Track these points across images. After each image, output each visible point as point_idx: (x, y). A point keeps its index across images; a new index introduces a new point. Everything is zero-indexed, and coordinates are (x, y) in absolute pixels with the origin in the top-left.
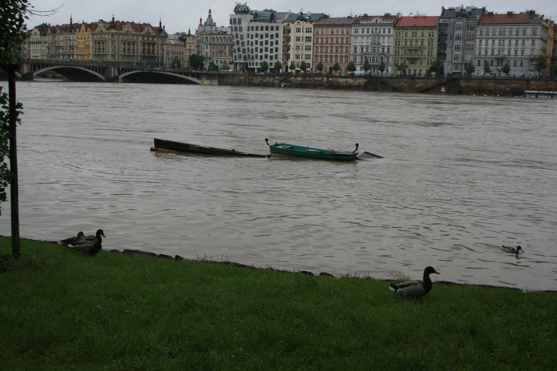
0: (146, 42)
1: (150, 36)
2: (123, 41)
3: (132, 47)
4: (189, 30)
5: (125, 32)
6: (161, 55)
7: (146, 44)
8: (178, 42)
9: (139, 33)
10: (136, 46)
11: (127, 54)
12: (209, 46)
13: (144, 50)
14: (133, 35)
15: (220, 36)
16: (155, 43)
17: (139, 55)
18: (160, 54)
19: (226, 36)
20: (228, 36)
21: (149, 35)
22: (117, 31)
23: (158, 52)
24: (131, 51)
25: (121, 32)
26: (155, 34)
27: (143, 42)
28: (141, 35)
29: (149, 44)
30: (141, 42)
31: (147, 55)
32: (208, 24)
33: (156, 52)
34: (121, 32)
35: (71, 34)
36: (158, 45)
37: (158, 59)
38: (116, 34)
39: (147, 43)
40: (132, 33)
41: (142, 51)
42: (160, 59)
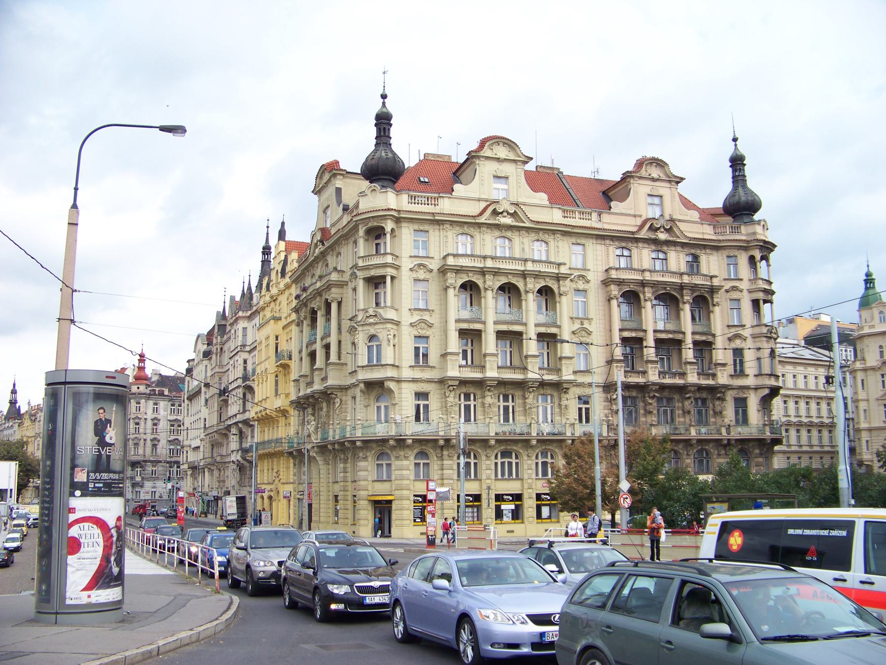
0: (643, 284)
1: (667, 243)
2: (459, 270)
4: (868, 275)
5: (473, 209)
6: (759, 375)
7: (649, 293)
9: (593, 222)
10: (566, 306)
11: (492, 373)
13: (633, 344)
14: (542, 230)
16: (713, 290)
18: (750, 367)
21: (662, 236)
23: (738, 353)
25: (446, 206)
26: (707, 232)
27: (620, 282)
28: (602, 237)
30: (606, 283)
31: (653, 376)
33: (722, 354)
34: (446, 206)
37: (741, 404)
38: (398, 220)
39: (654, 285)
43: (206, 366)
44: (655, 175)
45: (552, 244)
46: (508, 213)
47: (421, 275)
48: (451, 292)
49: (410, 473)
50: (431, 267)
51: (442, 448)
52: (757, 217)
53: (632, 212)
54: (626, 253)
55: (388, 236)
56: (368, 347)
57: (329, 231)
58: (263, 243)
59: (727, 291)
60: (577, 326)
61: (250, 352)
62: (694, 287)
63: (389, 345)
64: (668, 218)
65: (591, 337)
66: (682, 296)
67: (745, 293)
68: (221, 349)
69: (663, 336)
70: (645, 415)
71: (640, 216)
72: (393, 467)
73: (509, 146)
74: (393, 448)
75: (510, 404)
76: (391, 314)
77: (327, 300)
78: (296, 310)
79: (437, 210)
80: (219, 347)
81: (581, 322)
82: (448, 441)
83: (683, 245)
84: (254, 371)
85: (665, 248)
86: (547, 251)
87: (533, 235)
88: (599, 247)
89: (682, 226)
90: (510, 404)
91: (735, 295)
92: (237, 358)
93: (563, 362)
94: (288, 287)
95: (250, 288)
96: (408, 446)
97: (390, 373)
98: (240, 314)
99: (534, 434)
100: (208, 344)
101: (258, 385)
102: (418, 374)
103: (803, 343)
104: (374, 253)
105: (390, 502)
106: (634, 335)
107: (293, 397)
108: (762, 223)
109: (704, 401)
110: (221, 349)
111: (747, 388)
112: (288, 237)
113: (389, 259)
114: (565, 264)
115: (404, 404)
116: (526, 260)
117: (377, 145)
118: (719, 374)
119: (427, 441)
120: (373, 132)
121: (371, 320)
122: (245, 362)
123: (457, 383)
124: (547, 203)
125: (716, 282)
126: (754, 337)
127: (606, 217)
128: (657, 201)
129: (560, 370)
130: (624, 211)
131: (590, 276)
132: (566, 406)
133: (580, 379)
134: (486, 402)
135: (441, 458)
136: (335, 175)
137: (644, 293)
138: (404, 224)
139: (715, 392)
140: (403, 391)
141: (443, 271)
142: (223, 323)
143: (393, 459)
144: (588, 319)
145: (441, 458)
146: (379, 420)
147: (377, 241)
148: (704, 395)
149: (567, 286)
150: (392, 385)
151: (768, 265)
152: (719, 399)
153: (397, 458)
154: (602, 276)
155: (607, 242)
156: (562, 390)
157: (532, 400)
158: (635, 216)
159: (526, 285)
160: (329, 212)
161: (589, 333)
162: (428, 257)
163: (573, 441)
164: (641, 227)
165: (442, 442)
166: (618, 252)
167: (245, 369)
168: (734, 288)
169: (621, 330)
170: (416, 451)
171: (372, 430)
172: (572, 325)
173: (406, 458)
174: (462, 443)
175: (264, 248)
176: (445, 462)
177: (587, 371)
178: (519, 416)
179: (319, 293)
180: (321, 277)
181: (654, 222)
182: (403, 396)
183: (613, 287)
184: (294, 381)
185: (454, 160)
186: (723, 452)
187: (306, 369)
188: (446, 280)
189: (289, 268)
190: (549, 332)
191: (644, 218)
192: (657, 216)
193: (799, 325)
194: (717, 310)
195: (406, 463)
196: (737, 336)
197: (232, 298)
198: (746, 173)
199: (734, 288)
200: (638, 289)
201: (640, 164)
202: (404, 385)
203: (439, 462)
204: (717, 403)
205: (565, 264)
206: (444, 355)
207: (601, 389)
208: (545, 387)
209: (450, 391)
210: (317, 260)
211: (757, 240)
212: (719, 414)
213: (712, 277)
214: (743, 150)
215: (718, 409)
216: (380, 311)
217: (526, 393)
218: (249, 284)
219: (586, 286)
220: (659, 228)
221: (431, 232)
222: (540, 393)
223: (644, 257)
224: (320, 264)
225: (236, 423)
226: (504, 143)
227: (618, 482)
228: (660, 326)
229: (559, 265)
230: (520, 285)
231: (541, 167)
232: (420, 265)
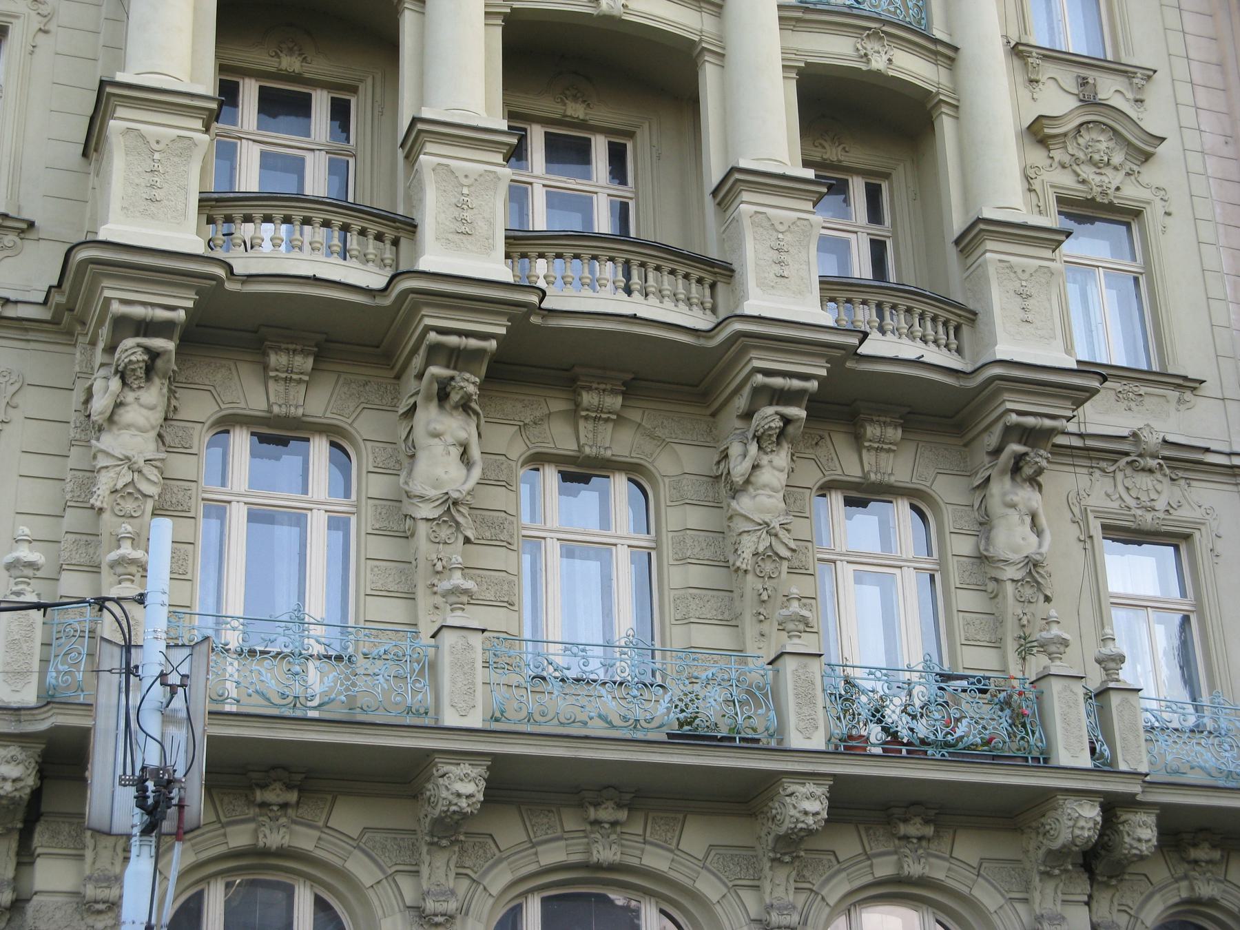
65: (1152, 174)
81: (1084, 82)
93: (993, 253)
129: (972, 317)
132: (1033, 565)
134: (417, 487)
156: (997, 452)
157: (777, 502)
163: (1113, 806)
172: (1024, 93)
178: (686, 622)
190: (878, 63)
208: (872, 431)
209: (123, 376)
217: (735, 450)
222: (836, 475)
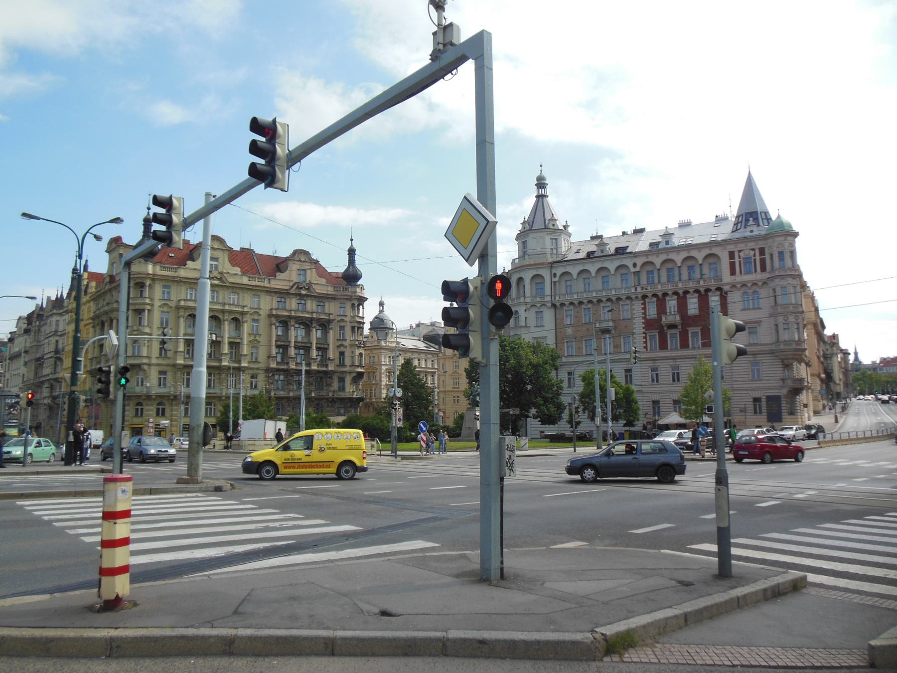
0: (290, 317)
1: (306, 295)
3: (227, 330)
8: (421, 345)
10: (246, 328)
12: (548, 316)
13: (283, 347)
14: (236, 288)
15: (598, 265)
16: (329, 321)
17: (261, 366)
18: (348, 361)
19: (629, 263)
20: (640, 261)
21: (304, 292)
22: (159, 271)
23: (342, 354)
24: (226, 349)
25: (182, 273)
26: (330, 290)
27: (277, 316)
28: (270, 292)
29: (306, 324)
30: (270, 316)
32: (538, 225)
34: (182, 273)
35: (61, 314)
36: (342, 328)
37: (342, 380)
38: (153, 280)
40: (231, 280)
41: (274, 351)
42: (348, 379)
43: (26, 339)
44: (302, 259)
45: (241, 294)
46: (217, 278)
47: (165, 309)
48: (182, 320)
49: (154, 413)
50: (171, 305)
51: (172, 400)
52: (359, 283)
53: (288, 279)
54: (283, 300)
55: (147, 288)
56: (133, 346)
57: (115, 279)
58: (73, 266)
59: (338, 321)
60: (252, 338)
61: (61, 336)
62: (318, 320)
63: (144, 346)
64: (308, 282)
66: (312, 324)
67: (348, 323)
68: (39, 330)
69: (300, 345)
70: (287, 385)
71: (292, 281)
72: (144, 410)
73: (221, 241)
74: (145, 400)
75: (213, 378)
76: (147, 330)
77: (110, 317)
78: (93, 319)
79: (176, 274)
80: (37, 328)
82: (175, 397)
83: (315, 297)
84: (63, 349)
85: (305, 298)
86: (238, 298)
87: (231, 289)
88: (267, 297)
89: (314, 286)
90: (213, 378)
91: (342, 324)
92: (51, 339)
94: (88, 302)
95: (62, 295)
96: (154, 399)
97: (145, 361)
98: (55, 311)
99: (224, 394)
100: (28, 324)
101: (66, 358)
102: (161, 361)
103: (422, 339)
104: (139, 296)
105: (141, 428)
106: (283, 343)
107: (89, 369)
108: (361, 286)
109: (321, 378)
110: (39, 330)
111: (345, 372)
112: (90, 270)
113: (147, 301)
114: (247, 306)
115: (152, 377)
116: (225, 304)
117: (144, 236)
118: (329, 365)
119: (164, 396)
120: (142, 228)
121: (135, 333)
122: (57, 342)
123: (182, 367)
124: (240, 273)
125: (332, 317)
126: (351, 346)
127: (273, 282)
128: (302, 272)
130: (283, 278)
131: (261, 312)
133: (252, 366)
135: (172, 405)
136: (119, 246)
137: (290, 322)
138: (157, 282)
139: (328, 374)
140: (152, 370)
141: (178, 308)
142: (41, 313)
143: (144, 405)
144: (258, 334)
145: (172, 405)
146: (138, 385)
147: (141, 289)
148: (322, 375)
149: (247, 318)
150: (145, 367)
151: (363, 308)
152: (329, 377)
153: (147, 405)
154: (268, 313)
155: (273, 294)
158: (289, 281)
159: (224, 317)
160: (115, 265)
161: (259, 342)
162: (170, 300)
164: (292, 287)
165: (172, 397)
166: (279, 300)
167: (57, 346)
168: (342, 320)
169: (276, 341)
170: (157, 402)
171: (133, 390)
173: (152, 405)
174: (182, 398)
175: (73, 269)
176: (174, 408)
177: (256, 362)
179: (106, 313)
180: (108, 304)
181: (300, 284)
182: (152, 372)
183: (273, 319)
184: (90, 359)
185: (191, 242)
186: (330, 405)
187: (96, 354)
188: (179, 313)
189: (89, 291)
191: (294, 282)
192: (301, 281)
193: (421, 328)
194: (331, 331)
195: (151, 408)
196: (342, 345)
197: (49, 298)
198: (356, 259)
199: (342, 320)
200: (288, 319)
201: (295, 252)
202: (153, 367)
203: (170, 408)
204: (328, 379)
205: (247, 306)
206: (176, 352)
207: (263, 372)
210: (106, 292)
211: (357, 296)
212: (329, 385)
213: (329, 314)
214: (355, 246)
215: (329, 383)
216: (141, 328)
218: (62, 292)
219: (259, 318)
220: (302, 288)
221: (173, 287)
223: (293, 303)
224: (109, 294)
225: (49, 380)
226: (217, 240)
227: (238, 419)
228: (300, 339)
229: (244, 307)
230: (221, 316)
231: (243, 248)
232: (165, 304)
